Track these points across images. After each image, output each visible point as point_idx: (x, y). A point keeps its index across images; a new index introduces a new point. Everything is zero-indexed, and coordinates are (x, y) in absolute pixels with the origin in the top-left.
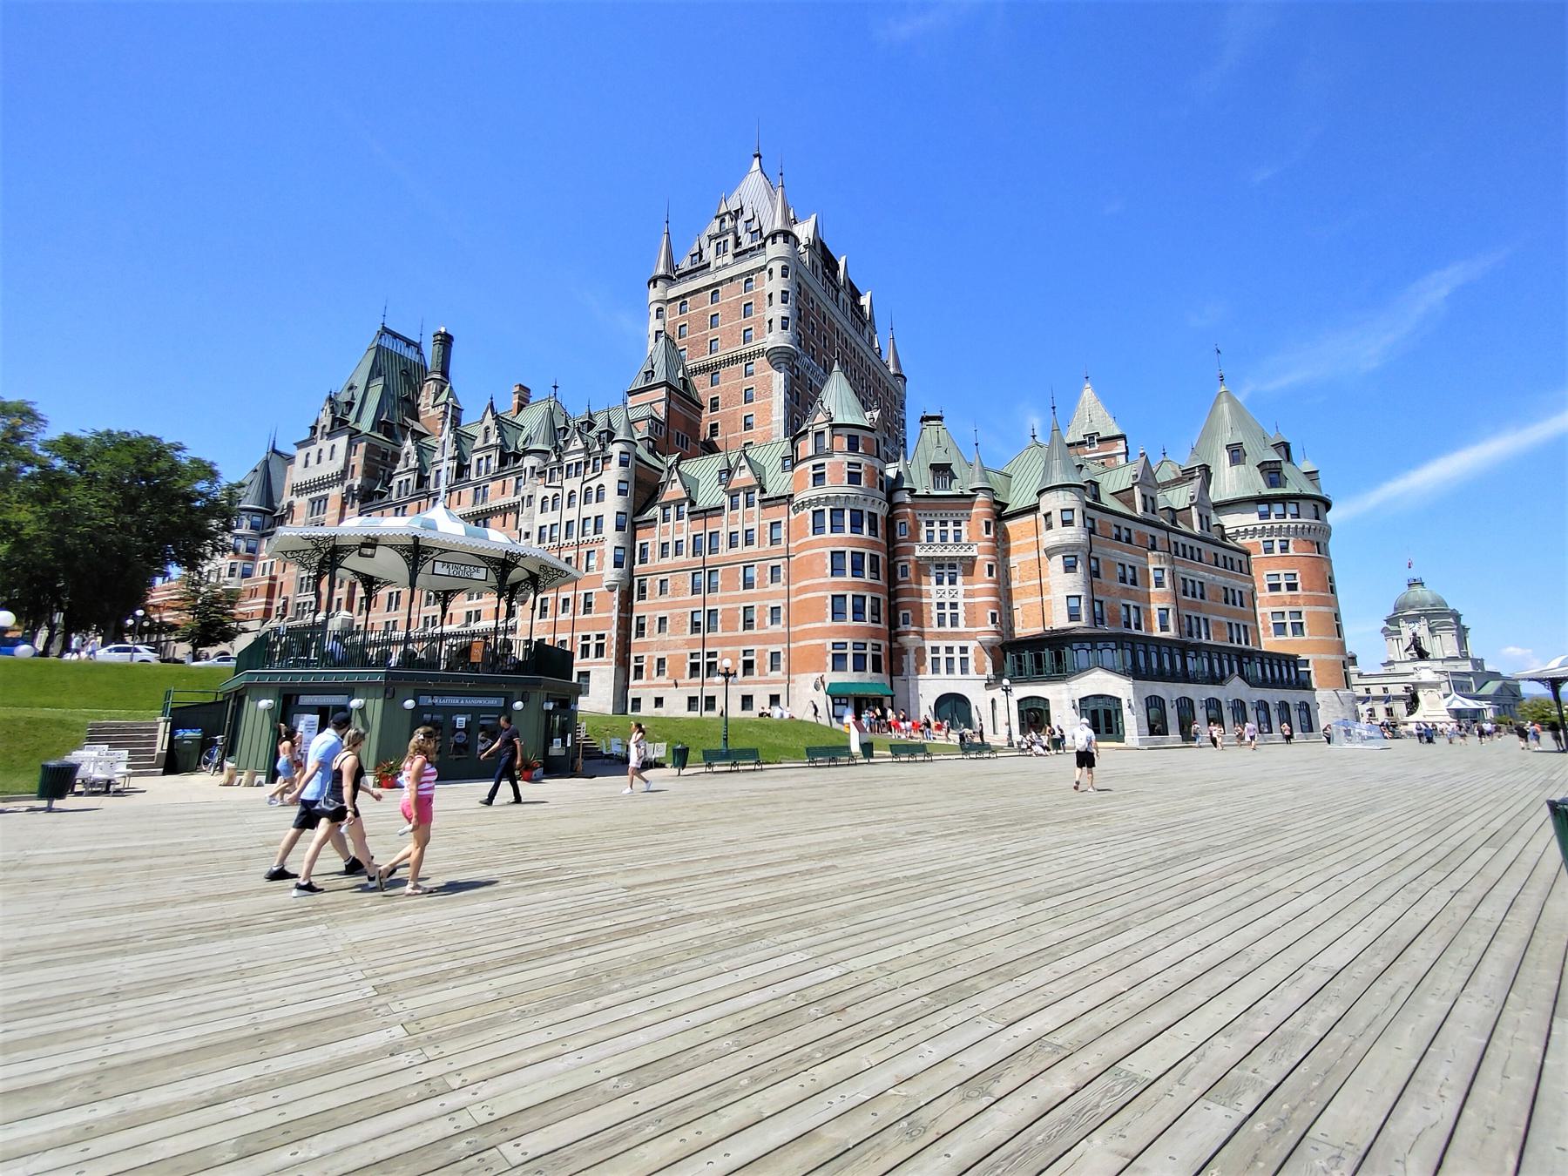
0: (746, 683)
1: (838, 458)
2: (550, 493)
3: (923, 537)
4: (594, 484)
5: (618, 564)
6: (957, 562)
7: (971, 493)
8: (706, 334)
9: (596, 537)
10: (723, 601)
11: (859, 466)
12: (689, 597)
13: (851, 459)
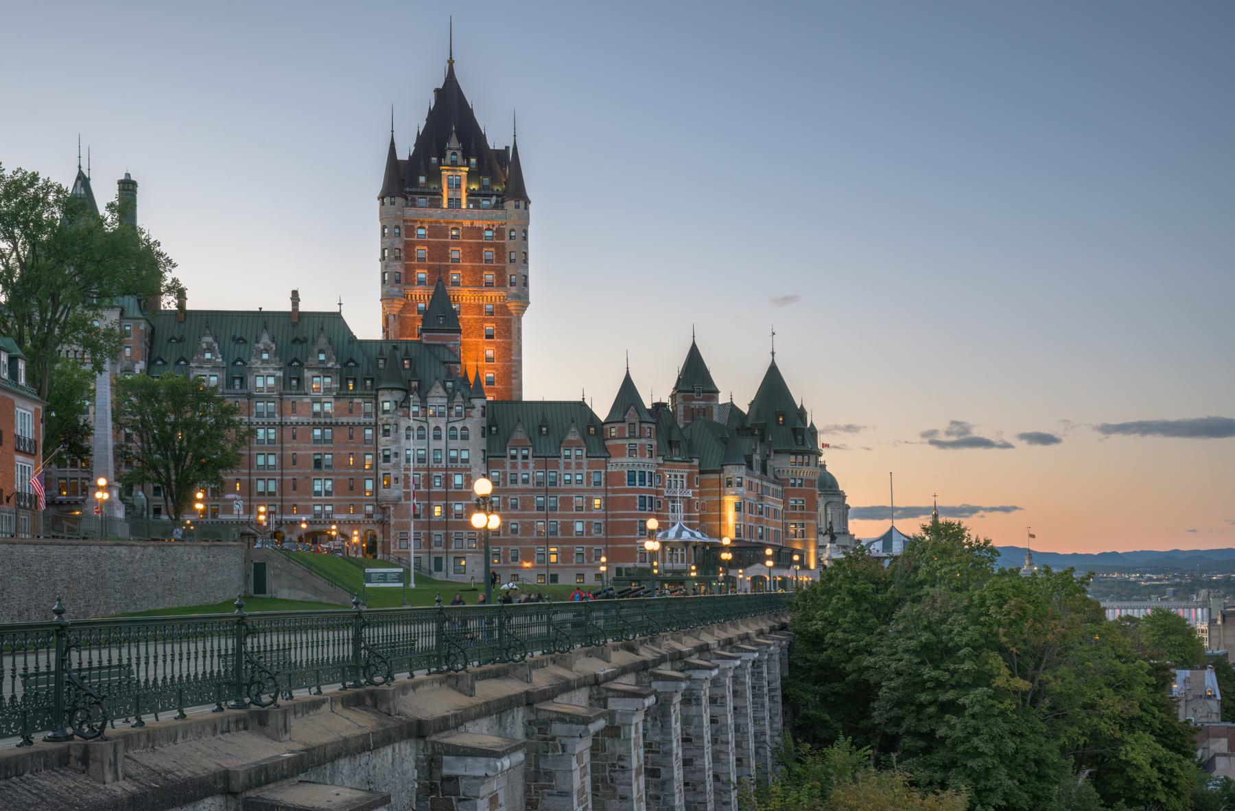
1: (643, 441)
4: (459, 426)
7: (688, 460)
8: (447, 266)
9: (464, 465)
10: (560, 516)
11: (651, 446)
12: (536, 512)
13: (649, 443)
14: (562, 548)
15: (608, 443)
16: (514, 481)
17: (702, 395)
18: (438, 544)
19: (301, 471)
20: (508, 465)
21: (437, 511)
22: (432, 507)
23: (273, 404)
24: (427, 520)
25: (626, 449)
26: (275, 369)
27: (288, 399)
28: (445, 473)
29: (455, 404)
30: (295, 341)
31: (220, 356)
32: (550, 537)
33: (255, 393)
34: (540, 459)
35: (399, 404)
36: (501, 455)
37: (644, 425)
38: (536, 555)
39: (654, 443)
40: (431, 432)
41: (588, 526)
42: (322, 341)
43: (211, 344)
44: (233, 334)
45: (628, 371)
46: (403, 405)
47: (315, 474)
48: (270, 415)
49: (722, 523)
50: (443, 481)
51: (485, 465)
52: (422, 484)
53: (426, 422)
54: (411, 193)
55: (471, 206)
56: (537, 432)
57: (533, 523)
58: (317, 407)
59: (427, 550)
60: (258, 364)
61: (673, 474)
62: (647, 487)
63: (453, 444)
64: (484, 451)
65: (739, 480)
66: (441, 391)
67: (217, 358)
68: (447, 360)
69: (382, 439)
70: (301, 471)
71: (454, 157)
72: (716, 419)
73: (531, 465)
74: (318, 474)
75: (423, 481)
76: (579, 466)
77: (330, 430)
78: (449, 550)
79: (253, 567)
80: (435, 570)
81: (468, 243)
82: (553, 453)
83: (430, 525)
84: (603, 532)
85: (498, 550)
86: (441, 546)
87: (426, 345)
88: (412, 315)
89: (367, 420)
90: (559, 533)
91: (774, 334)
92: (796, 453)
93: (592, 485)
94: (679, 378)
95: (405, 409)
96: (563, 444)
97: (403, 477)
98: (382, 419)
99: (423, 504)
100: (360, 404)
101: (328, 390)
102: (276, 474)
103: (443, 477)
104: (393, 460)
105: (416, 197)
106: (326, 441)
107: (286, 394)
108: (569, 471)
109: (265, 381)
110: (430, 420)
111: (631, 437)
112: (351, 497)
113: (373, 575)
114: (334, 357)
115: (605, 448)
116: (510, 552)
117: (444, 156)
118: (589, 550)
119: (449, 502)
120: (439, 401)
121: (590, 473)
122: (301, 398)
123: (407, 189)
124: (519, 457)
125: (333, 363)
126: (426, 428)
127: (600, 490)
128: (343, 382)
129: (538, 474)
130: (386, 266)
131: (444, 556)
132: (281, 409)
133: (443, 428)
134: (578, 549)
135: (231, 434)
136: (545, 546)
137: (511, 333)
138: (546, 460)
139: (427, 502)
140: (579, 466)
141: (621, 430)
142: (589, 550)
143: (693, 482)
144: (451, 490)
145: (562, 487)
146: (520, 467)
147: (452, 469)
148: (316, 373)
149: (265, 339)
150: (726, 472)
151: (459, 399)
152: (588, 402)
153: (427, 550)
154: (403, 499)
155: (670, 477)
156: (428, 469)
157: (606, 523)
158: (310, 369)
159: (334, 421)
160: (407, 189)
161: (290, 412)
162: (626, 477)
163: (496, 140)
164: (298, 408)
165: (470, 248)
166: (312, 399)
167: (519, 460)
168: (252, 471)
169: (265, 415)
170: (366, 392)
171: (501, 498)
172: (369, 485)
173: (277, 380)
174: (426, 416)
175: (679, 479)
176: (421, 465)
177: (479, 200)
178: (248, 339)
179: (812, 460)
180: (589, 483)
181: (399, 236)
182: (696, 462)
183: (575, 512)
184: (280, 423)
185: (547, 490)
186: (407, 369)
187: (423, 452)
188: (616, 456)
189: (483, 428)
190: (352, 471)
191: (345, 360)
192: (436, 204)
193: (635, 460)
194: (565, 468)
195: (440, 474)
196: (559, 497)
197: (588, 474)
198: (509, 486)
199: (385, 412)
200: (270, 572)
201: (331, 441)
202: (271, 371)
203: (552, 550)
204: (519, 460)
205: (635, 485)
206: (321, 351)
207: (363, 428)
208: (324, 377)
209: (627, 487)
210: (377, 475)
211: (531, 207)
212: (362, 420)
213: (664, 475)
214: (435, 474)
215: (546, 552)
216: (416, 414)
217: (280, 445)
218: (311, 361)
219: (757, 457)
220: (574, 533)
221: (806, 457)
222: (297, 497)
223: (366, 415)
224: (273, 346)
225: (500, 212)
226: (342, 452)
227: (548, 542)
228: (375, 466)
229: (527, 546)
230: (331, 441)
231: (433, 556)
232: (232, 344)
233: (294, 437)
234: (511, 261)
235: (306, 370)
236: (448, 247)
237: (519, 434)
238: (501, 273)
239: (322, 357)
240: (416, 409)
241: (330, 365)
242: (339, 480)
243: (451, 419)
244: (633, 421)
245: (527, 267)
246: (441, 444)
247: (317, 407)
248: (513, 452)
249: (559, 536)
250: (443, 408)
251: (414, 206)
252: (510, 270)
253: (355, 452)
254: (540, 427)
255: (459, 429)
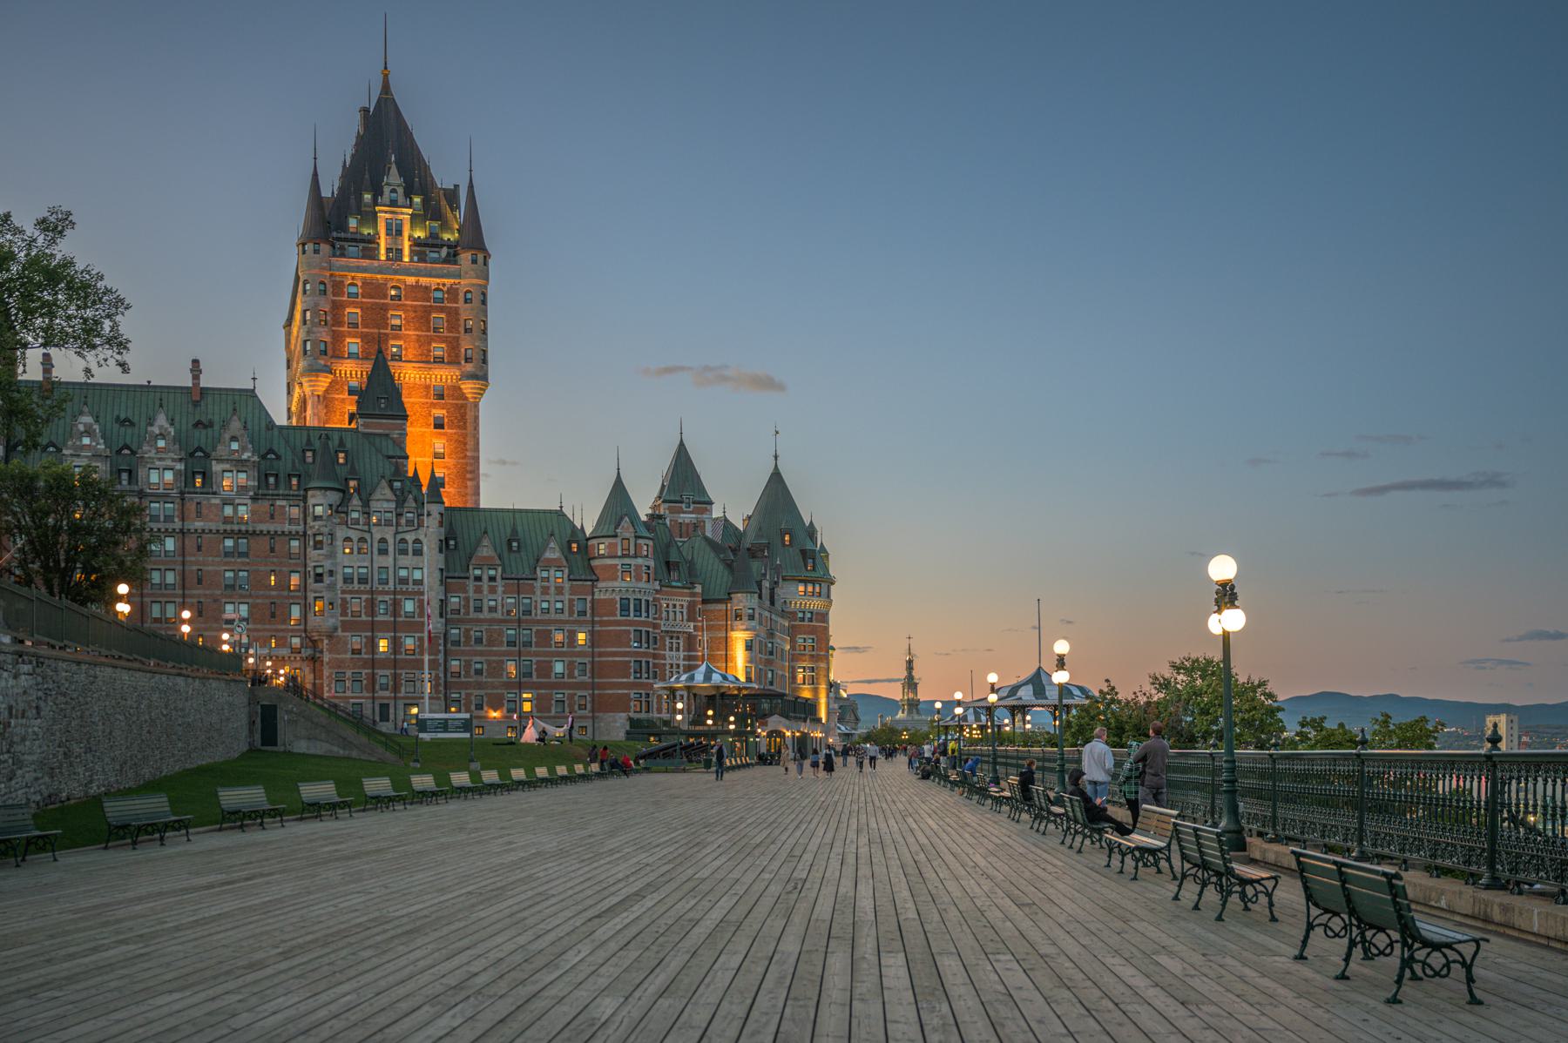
0: (559, 718)
1: (640, 561)
2: (355, 535)
3: (664, 614)
5: (441, 616)
6: (680, 635)
7: (689, 585)
8: (385, 334)
9: (416, 588)
10: (536, 654)
11: (648, 568)
14: (538, 695)
15: (595, 563)
16: (479, 609)
17: (692, 506)
18: (384, 687)
19: (208, 592)
20: (471, 589)
21: (383, 645)
22: (376, 640)
23: (171, 505)
24: (371, 656)
25: (618, 570)
26: (174, 460)
27: (192, 499)
28: (392, 597)
29: (406, 510)
30: (198, 424)
31: (102, 441)
32: (523, 680)
33: (149, 491)
34: (512, 581)
35: (334, 508)
36: (462, 575)
37: (640, 541)
38: (505, 702)
39: (652, 564)
40: (376, 545)
41: (570, 667)
42: (236, 426)
43: (91, 425)
44: (116, 413)
45: (619, 473)
46: (340, 509)
47: (226, 596)
48: (169, 519)
49: (730, 664)
50: (391, 608)
51: (443, 588)
52: (363, 611)
53: (369, 531)
54: (339, 239)
55: (416, 258)
56: (505, 548)
57: (502, 662)
58: (228, 511)
59: (371, 695)
60: (152, 454)
61: (671, 603)
62: (643, 619)
63: (404, 560)
64: (441, 570)
65: (751, 611)
66: (388, 493)
67: (98, 444)
68: (391, 453)
69: (313, 554)
70: (208, 592)
71: (394, 195)
72: (709, 534)
73: (500, 589)
74: (230, 597)
75: (365, 607)
76: (559, 590)
77: (245, 541)
78: (398, 695)
79: (259, 711)
80: (381, 720)
81: (412, 306)
82: (527, 573)
83: (373, 663)
84: (588, 674)
85: (458, 695)
86: (387, 689)
87: (365, 434)
88: (341, 396)
89: (294, 528)
90: (534, 674)
91: (777, 432)
92: (805, 582)
93: (576, 615)
94: (663, 486)
95: (343, 515)
96: (540, 564)
97: (340, 601)
98: (313, 527)
99: (366, 637)
100: (284, 507)
101: (242, 489)
102: (175, 596)
103: (389, 602)
104: (327, 580)
105: (346, 244)
106: (241, 555)
107: (189, 493)
108: (547, 598)
109: (161, 477)
110: (374, 530)
111: (624, 556)
112: (274, 627)
113: (429, 723)
114: (250, 446)
115: (592, 569)
116: (473, 698)
117: (382, 194)
118: (571, 696)
119: (398, 634)
120: (385, 505)
121: (573, 600)
122: (208, 499)
123: (335, 234)
124: (485, 578)
125: (250, 454)
126: (369, 541)
127: (585, 622)
128: (263, 478)
129: (509, 600)
130: (308, 332)
131: (392, 703)
132: (183, 513)
133: (391, 541)
134: (558, 696)
135: (133, 543)
136: (517, 691)
137: (465, 423)
138: (519, 583)
139: (370, 634)
140: (559, 590)
141: (610, 546)
142: (571, 696)
143: (695, 613)
144: (401, 619)
145: (539, 617)
146: (485, 593)
147: (402, 593)
148: (227, 466)
149: (161, 420)
150: (735, 601)
151: (411, 503)
152: (568, 512)
153: (371, 695)
154: (340, 630)
155: (668, 606)
156: (372, 592)
157: (593, 663)
158: (220, 461)
159: (250, 529)
160: (335, 234)
161: (195, 515)
162: (618, 606)
163: (444, 177)
164: (205, 511)
165: (415, 312)
166: (222, 499)
167: (485, 584)
168: (145, 591)
169: (162, 519)
170: (291, 493)
171: (462, 630)
172: (296, 612)
173: (177, 474)
174: (369, 525)
175: (678, 609)
176: (362, 587)
177: (425, 252)
178: (136, 420)
179: (824, 591)
180: (571, 613)
181: (325, 294)
182: (698, 589)
183: (553, 649)
184: (182, 531)
185: (519, 621)
186: (342, 464)
187: (365, 570)
188: (604, 580)
189: (441, 541)
190: (274, 593)
191: (263, 451)
192: (371, 254)
193: (630, 585)
194: (542, 593)
195: (387, 598)
196: (534, 629)
197: (571, 601)
198: (473, 615)
199: (316, 518)
200: (283, 717)
201: (246, 555)
202: (169, 463)
203: (525, 696)
204: (485, 584)
205: (629, 615)
206: (234, 439)
207: (287, 538)
208: (238, 471)
209: (619, 618)
210: (306, 598)
211: (491, 262)
212: (287, 528)
213: (661, 606)
214: (380, 598)
215: (518, 699)
216: (357, 522)
217: (180, 559)
218: (221, 450)
219: (766, 584)
220: (553, 675)
221: (817, 587)
222: (203, 626)
223: (291, 521)
224: (172, 430)
225: (453, 268)
226: (262, 568)
227: (521, 686)
228: (304, 587)
229: (495, 691)
230: (246, 555)
231: (377, 702)
232: (116, 426)
233: (199, 548)
234: (466, 331)
235: (214, 462)
236: (386, 310)
237: (485, 549)
238: (454, 345)
239: (235, 446)
240: (355, 515)
241: (245, 456)
242: (258, 604)
243: (400, 529)
244: (627, 535)
245: (486, 340)
246: (388, 561)
247: (228, 511)
248: (478, 572)
249: (535, 679)
250: (390, 515)
251: (343, 255)
252: (466, 344)
253: (277, 569)
254: (509, 542)
255: (410, 542)
